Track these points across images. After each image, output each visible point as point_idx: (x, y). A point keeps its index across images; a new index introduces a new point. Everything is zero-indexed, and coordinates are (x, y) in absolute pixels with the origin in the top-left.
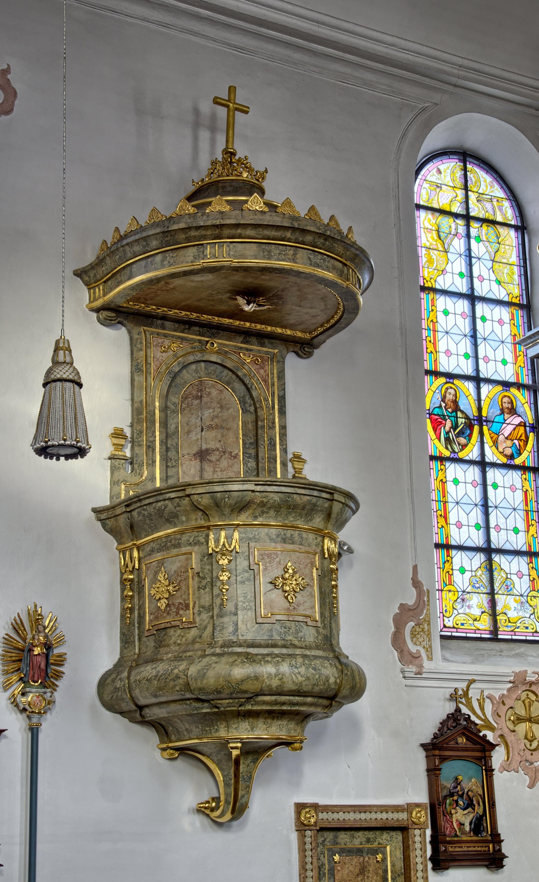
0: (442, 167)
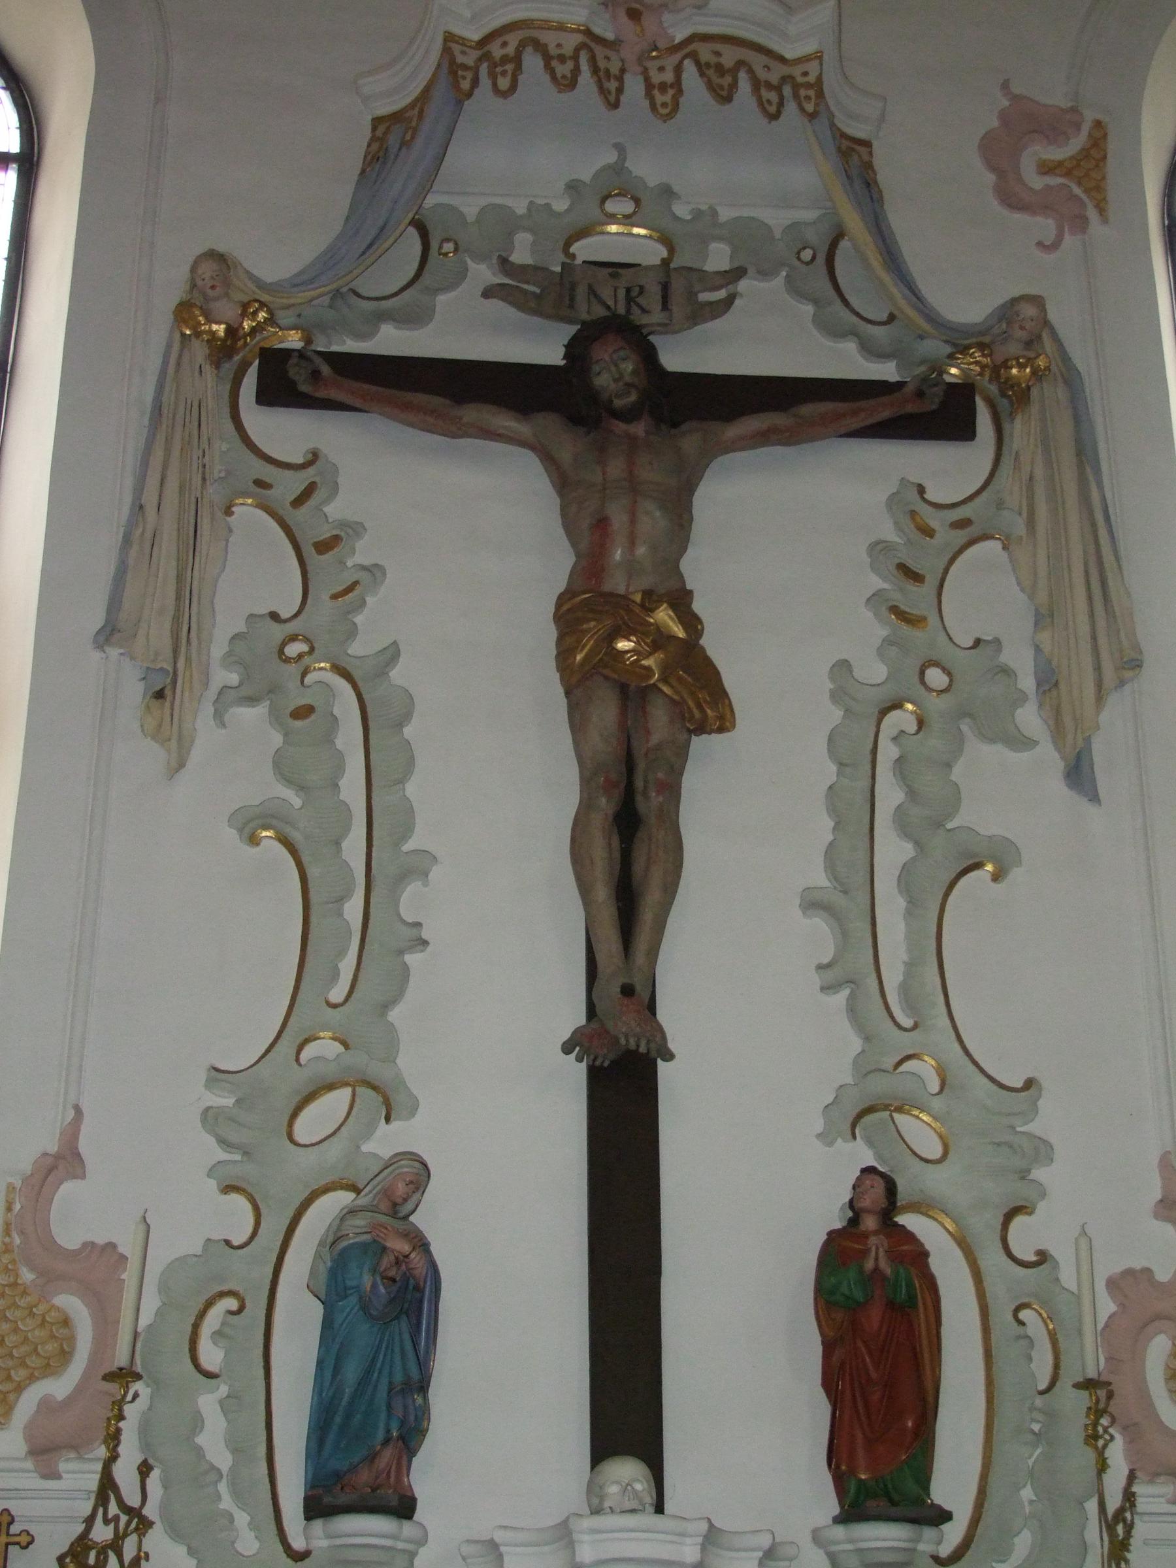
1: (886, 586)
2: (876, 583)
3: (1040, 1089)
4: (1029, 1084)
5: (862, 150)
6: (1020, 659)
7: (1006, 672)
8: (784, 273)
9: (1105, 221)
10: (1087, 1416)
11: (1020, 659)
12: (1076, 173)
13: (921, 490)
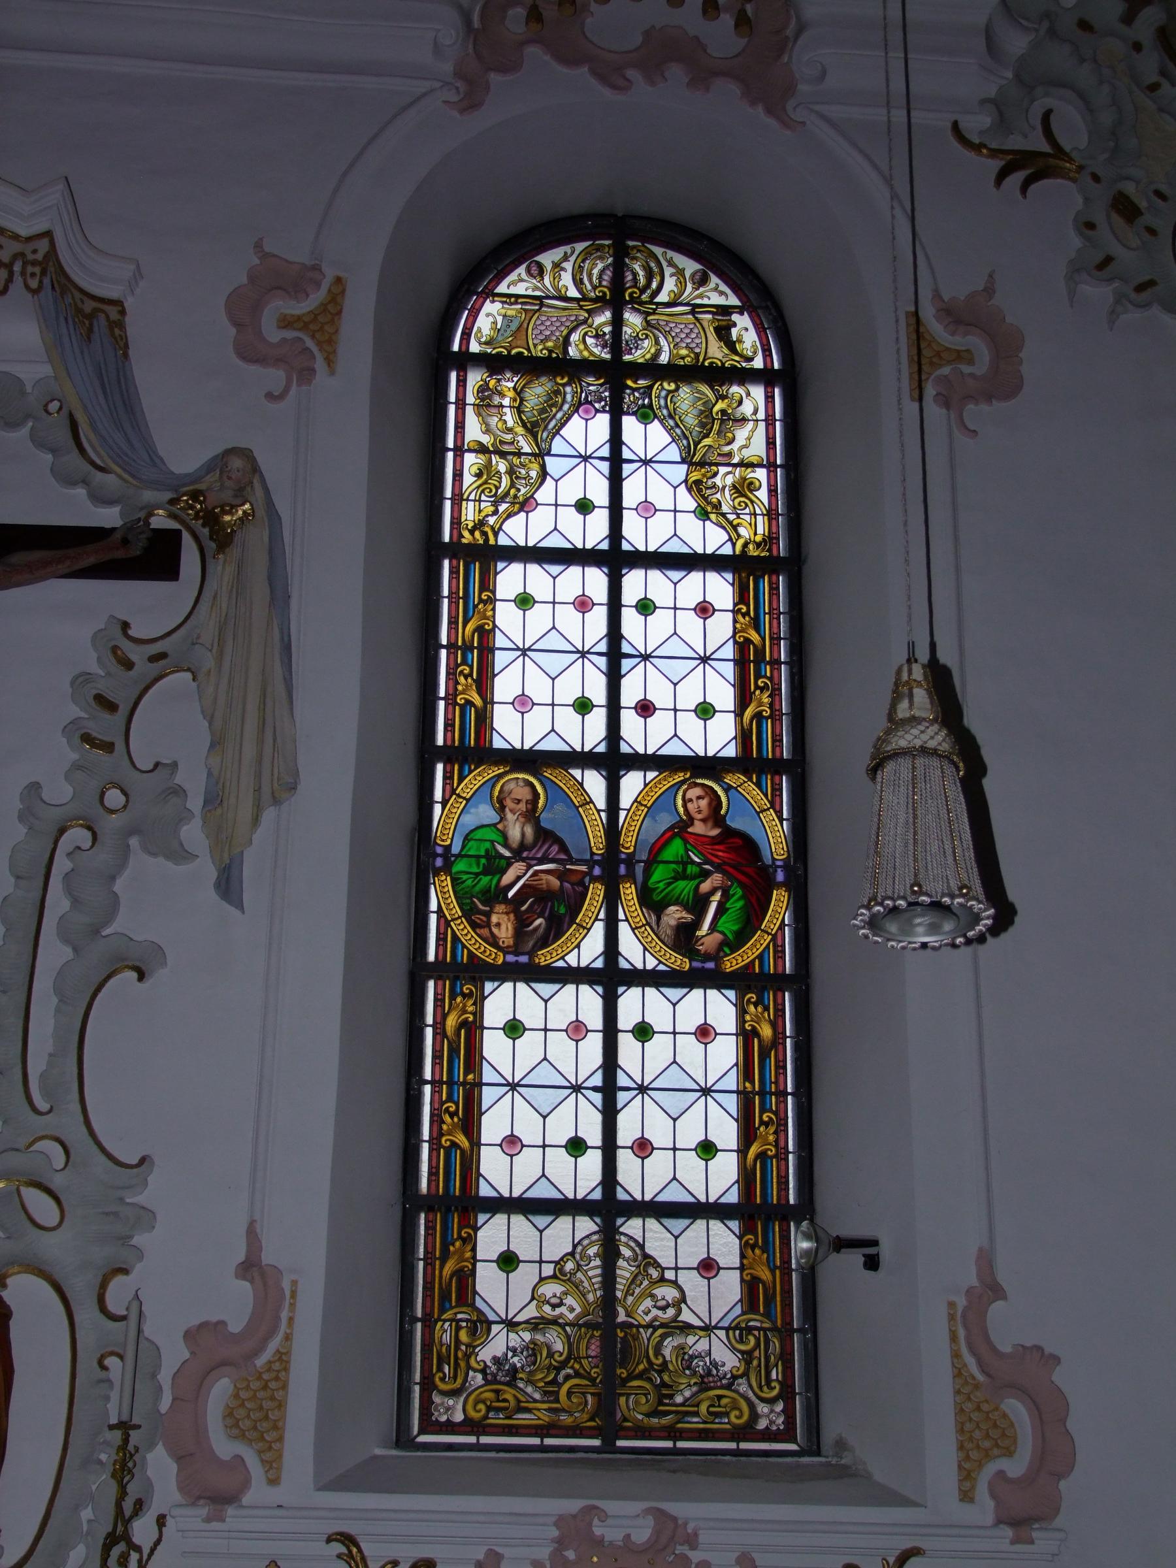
0: (547, 259)
1: (83, 715)
2: (75, 711)
3: (153, 1163)
4: (143, 1160)
5: (113, 312)
6: (193, 782)
7: (179, 792)
8: (30, 424)
9: (332, 372)
10: (117, 1454)
11: (193, 782)
12: (311, 327)
13: (125, 626)
